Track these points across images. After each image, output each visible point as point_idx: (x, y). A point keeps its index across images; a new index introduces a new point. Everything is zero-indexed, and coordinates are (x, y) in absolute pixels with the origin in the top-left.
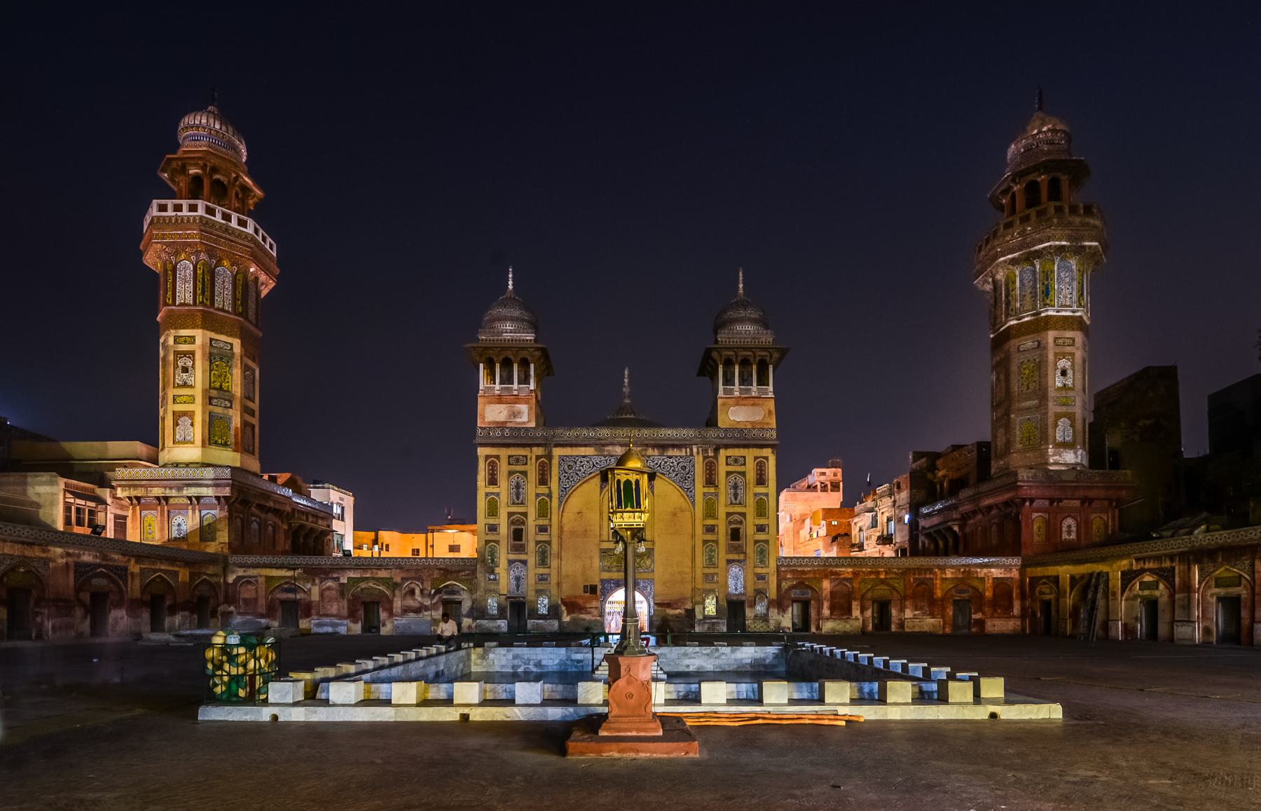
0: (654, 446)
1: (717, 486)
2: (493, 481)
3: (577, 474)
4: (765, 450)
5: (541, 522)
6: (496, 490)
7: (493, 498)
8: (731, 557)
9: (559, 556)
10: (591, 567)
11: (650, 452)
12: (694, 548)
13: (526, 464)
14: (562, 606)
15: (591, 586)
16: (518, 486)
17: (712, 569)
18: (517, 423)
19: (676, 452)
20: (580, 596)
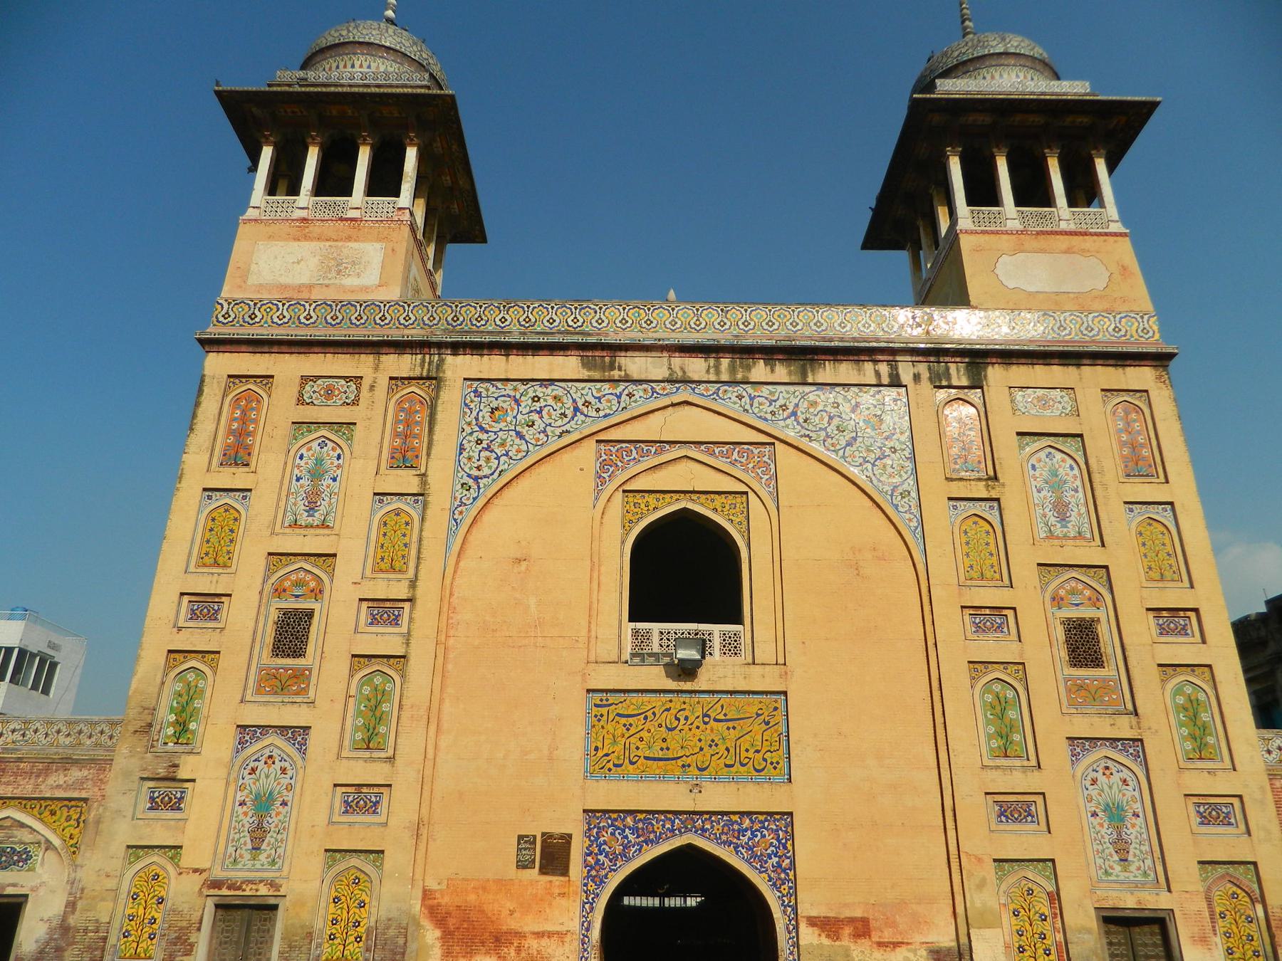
0: (770, 353)
1: (996, 478)
2: (237, 455)
3: (520, 436)
4: (1130, 371)
5: (381, 589)
6: (238, 478)
7: (227, 509)
8: (1083, 726)
9: (433, 717)
10: (551, 759)
11: (760, 371)
12: (936, 688)
13: (355, 402)
14: (426, 923)
15: (543, 834)
16: (317, 473)
17: (1018, 775)
18: (342, 288)
19: (845, 371)
20: (499, 882)
